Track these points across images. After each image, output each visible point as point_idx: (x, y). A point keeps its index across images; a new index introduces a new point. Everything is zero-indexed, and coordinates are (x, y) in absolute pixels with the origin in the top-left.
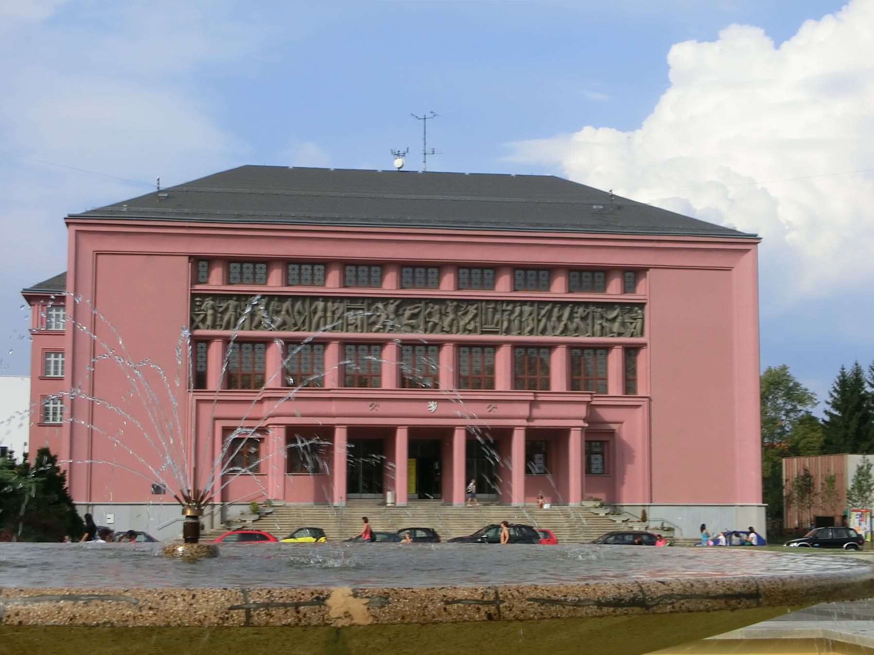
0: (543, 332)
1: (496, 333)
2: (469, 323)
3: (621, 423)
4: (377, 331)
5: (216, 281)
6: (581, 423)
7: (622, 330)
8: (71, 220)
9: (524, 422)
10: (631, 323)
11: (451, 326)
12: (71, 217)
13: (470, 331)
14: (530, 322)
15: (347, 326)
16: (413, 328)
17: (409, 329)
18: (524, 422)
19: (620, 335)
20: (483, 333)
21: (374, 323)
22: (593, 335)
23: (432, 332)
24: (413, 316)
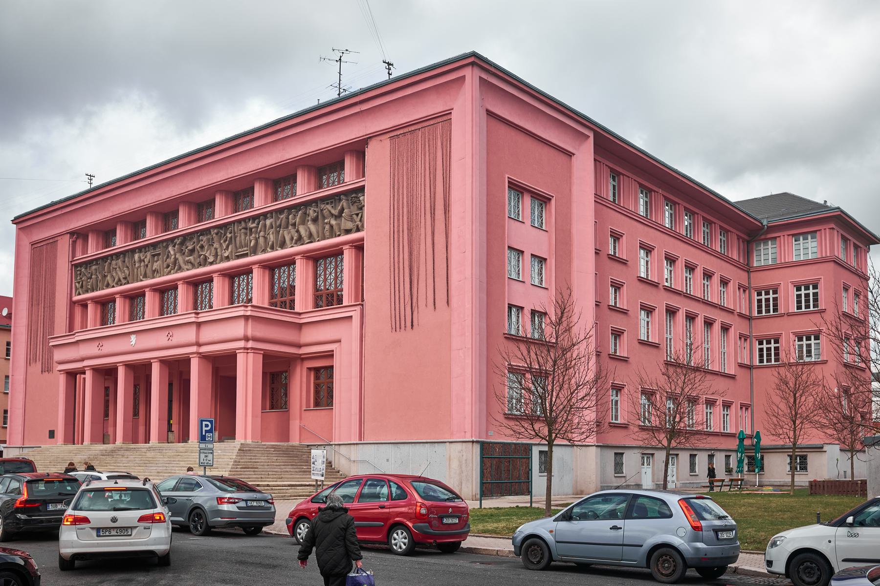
0: (283, 245)
1: (246, 255)
2: (227, 248)
3: (339, 341)
4: (169, 273)
5: (93, 249)
6: (242, 344)
7: (349, 225)
8: (17, 221)
9: (194, 349)
10: (357, 215)
11: (216, 255)
12: (16, 218)
13: (227, 259)
14: (271, 236)
15: (155, 273)
16: (193, 266)
17: (190, 266)
18: (194, 349)
19: (348, 232)
20: (238, 257)
21: (168, 266)
22: (324, 238)
23: (204, 265)
24: (192, 251)
